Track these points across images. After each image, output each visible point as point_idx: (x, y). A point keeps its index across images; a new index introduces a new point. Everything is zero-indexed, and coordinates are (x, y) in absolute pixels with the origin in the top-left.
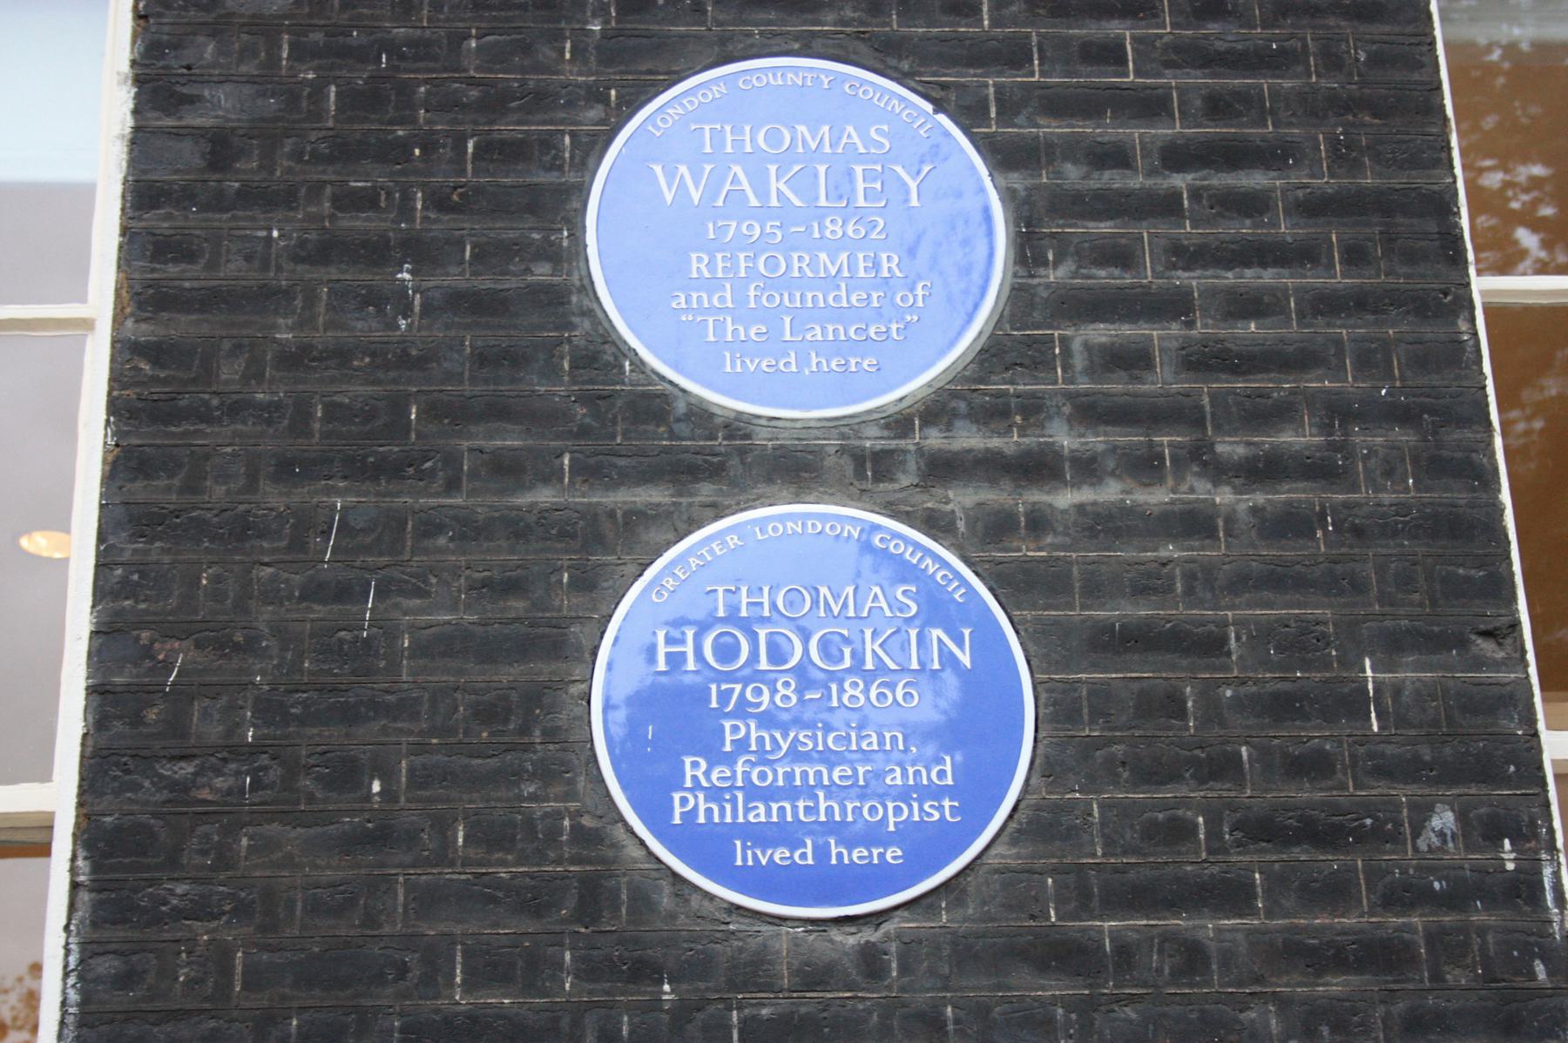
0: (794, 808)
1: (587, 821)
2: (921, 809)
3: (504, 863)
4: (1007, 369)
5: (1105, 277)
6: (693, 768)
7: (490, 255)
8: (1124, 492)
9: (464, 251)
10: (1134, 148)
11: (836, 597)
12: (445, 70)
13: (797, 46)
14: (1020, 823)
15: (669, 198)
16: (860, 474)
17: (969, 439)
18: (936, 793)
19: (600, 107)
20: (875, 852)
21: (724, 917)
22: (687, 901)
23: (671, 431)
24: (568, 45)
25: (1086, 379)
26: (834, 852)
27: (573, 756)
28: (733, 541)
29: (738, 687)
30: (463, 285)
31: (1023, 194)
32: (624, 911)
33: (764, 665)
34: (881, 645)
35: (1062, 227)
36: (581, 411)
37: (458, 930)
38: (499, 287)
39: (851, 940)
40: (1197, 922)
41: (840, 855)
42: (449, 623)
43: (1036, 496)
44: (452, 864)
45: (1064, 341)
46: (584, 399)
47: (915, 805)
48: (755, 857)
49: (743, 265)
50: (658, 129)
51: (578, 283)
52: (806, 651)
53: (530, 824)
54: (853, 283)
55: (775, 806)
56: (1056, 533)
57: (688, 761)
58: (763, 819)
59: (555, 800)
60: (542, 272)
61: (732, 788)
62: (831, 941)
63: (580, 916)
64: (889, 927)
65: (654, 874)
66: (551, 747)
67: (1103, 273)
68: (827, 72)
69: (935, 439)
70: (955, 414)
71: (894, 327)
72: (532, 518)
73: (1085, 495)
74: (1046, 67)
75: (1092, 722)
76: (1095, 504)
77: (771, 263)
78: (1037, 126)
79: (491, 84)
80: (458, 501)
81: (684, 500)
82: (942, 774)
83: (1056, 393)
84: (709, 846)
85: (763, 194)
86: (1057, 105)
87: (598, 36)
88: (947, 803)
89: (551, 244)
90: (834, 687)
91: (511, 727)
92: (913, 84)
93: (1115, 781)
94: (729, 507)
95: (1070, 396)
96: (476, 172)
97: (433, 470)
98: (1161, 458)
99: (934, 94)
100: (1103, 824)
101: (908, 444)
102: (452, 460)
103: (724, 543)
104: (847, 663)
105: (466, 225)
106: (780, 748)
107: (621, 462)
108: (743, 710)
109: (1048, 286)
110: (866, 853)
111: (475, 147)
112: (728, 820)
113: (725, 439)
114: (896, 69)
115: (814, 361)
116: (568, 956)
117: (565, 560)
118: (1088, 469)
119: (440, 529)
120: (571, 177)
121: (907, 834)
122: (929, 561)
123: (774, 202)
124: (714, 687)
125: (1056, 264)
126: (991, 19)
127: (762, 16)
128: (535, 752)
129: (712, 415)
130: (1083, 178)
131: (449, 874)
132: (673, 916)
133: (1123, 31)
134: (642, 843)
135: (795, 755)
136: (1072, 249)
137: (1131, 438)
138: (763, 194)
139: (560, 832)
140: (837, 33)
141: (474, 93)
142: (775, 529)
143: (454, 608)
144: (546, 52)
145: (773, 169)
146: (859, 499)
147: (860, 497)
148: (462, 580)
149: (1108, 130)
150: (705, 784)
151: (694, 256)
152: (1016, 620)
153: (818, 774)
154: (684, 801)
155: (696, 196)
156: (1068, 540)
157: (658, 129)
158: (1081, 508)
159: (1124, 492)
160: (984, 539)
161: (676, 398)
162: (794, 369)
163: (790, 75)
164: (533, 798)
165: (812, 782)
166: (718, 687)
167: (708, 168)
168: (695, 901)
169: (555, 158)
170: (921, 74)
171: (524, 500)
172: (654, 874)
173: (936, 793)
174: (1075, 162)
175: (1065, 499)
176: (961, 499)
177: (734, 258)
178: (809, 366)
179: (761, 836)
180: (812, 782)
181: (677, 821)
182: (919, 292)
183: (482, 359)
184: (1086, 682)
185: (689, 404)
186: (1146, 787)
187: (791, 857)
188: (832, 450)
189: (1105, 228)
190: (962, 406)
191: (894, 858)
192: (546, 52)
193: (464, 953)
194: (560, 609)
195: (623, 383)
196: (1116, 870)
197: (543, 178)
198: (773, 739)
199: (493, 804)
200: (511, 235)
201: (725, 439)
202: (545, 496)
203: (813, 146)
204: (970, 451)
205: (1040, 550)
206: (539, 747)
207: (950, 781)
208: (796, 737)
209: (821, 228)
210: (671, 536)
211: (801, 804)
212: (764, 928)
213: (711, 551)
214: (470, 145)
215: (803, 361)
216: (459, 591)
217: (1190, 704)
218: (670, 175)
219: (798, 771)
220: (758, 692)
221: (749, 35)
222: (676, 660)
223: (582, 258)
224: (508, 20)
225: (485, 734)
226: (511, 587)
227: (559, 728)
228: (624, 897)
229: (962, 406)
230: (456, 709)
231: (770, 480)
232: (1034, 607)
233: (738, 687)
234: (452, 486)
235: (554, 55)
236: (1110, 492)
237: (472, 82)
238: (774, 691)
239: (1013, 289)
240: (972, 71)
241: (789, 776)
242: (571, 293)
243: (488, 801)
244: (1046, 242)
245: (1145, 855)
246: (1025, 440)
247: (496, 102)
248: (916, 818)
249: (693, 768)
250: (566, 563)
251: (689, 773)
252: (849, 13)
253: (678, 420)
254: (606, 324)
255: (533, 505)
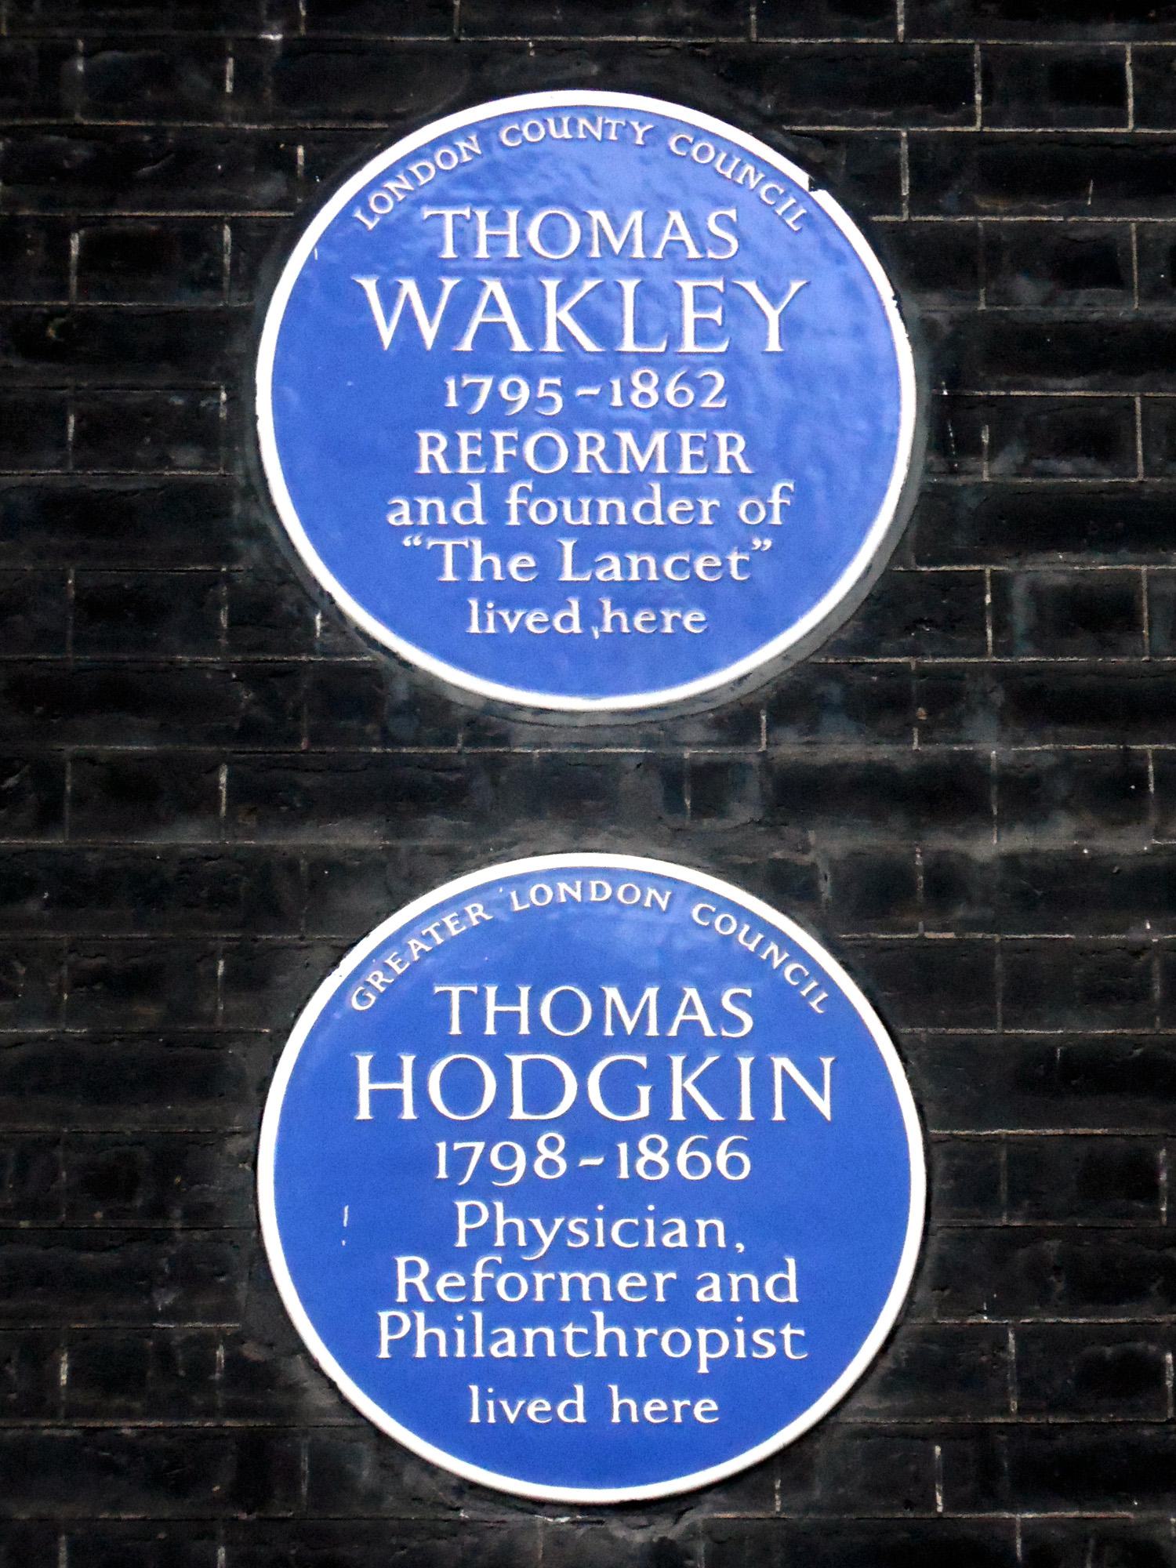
0: (560, 1338)
1: (252, 1352)
2: (749, 1340)
3: (128, 1413)
4: (908, 630)
5: (1070, 473)
6: (410, 1272)
7: (106, 433)
8: (1078, 835)
9: (65, 422)
10: (1129, 249)
11: (631, 1008)
12: (36, 112)
13: (595, 70)
14: (896, 1360)
15: (387, 334)
16: (673, 803)
17: (844, 747)
18: (770, 1314)
19: (279, 176)
20: (678, 1405)
21: (451, 1499)
22: (398, 1475)
23: (385, 731)
24: (230, 67)
25: (1029, 648)
26: (617, 1403)
27: (230, 1250)
28: (476, 913)
29: (479, 1147)
30: (64, 484)
31: (947, 330)
32: (304, 1489)
33: (518, 1113)
34: (696, 1083)
35: (1008, 386)
36: (247, 696)
37: (62, 1512)
38: (121, 487)
39: (639, 1537)
40: (1154, 1514)
41: (625, 1410)
42: (43, 1038)
43: (943, 841)
44: (52, 1414)
45: (1001, 584)
46: (255, 676)
47: (740, 1333)
48: (499, 1409)
49: (500, 452)
50: (371, 215)
51: (242, 482)
52: (583, 1091)
53: (165, 1354)
54: (673, 487)
55: (530, 1333)
56: (970, 900)
57: (402, 1261)
58: (511, 1352)
59: (205, 1319)
60: (186, 464)
61: (469, 1305)
62: (612, 1539)
63: (239, 1495)
64: (695, 1517)
65: (349, 1433)
66: (198, 1235)
67: (1066, 466)
68: (644, 116)
69: (790, 747)
70: (823, 704)
71: (734, 558)
72: (171, 871)
73: (1019, 840)
74: (995, 105)
75: (1014, 1203)
76: (1034, 853)
77: (545, 452)
78: (974, 211)
79: (111, 134)
80: (56, 841)
81: (403, 844)
82: (781, 1286)
83: (978, 670)
84: (426, 1390)
85: (533, 330)
86: (1012, 173)
87: (278, 52)
88: (787, 1331)
89: (199, 413)
90: (623, 1147)
91: (139, 1203)
92: (779, 138)
93: (1043, 1297)
94: (472, 855)
95: (1004, 675)
96: (84, 289)
97: (18, 789)
98: (1141, 779)
99: (811, 155)
100: (1020, 1363)
101: (748, 755)
102: (47, 775)
103: (463, 914)
104: (644, 1111)
105: (68, 381)
106: (540, 1243)
107: (308, 781)
108: (486, 1184)
109: (980, 487)
110: (663, 1407)
111: (84, 246)
112: (461, 1353)
113: (466, 744)
114: (753, 110)
115: (608, 616)
116: (222, 1553)
117: (223, 938)
118: (1026, 796)
119: (30, 887)
120: (234, 300)
121: (729, 1378)
122: (773, 947)
123: (552, 345)
124: (442, 1146)
125: (996, 447)
126: (907, 23)
127: (540, 17)
128: (172, 1243)
129: (448, 704)
130: (1044, 304)
131: (47, 1429)
132: (375, 1497)
133: (1122, 44)
134: (332, 1385)
135: (562, 1256)
136: (1020, 425)
137: (1092, 746)
138: (533, 330)
139: (212, 1363)
140: (657, 46)
141: (81, 152)
142: (541, 893)
143: (51, 1014)
144: (195, 80)
145: (551, 285)
146: (670, 845)
147: (673, 845)
148: (65, 971)
149: (1091, 219)
150: (426, 1297)
151: (424, 436)
152: (903, 1041)
153: (596, 1284)
154: (395, 1324)
155: (429, 333)
156: (990, 913)
157: (371, 215)
158: (1011, 861)
159: (1078, 835)
160: (856, 909)
161: (394, 675)
162: (576, 628)
163: (583, 122)
164: (170, 1314)
165: (586, 1297)
166: (450, 1146)
167: (449, 284)
168: (409, 1476)
169: (207, 266)
170: (790, 119)
171: (156, 841)
172: (349, 1433)
173: (770, 1314)
174: (1031, 272)
175: (989, 846)
176: (828, 845)
177: (489, 445)
178: (600, 623)
179: (515, 1377)
180: (586, 1297)
181: (384, 1353)
182: (776, 500)
183: (95, 607)
184: (1007, 1140)
185: (412, 685)
186: (1089, 1307)
187: (553, 1412)
188: (632, 763)
189: (1074, 389)
190: (834, 691)
191: (705, 1414)
192: (195, 80)
193: (73, 1548)
194: (211, 1019)
195: (311, 651)
196: (1037, 1432)
197: (188, 301)
198: (530, 1230)
199: (111, 1322)
200: (137, 397)
201: (466, 744)
202: (190, 836)
203: (617, 246)
204: (843, 766)
205: (945, 928)
206: (178, 1235)
207: (793, 1298)
208: (564, 1227)
209: (627, 389)
210: (380, 903)
211: (569, 1330)
212: (512, 1517)
213: (442, 929)
214: (75, 242)
215: (591, 617)
216: (60, 989)
217: (1163, 1177)
218: (388, 295)
219: (566, 1278)
220: (508, 1155)
221: (521, 49)
222: (386, 1102)
223: (248, 438)
224: (136, 24)
225: (99, 1215)
226: (132, 982)
227: (210, 1207)
228: (305, 1467)
229: (834, 691)
230: (55, 1176)
231: (534, 811)
232: (933, 1022)
233: (479, 1147)
234: (48, 817)
235: (206, 85)
236: (1058, 836)
237: (78, 133)
238: (532, 1153)
239: (923, 494)
240: (875, 114)
241: (552, 1287)
242: (231, 498)
243: (105, 1318)
244: (979, 413)
245: (1082, 1412)
246: (929, 748)
247: (114, 169)
248: (741, 1353)
249: (410, 1272)
250: (223, 945)
251: (403, 1280)
252: (683, 13)
253: (397, 712)
254: (285, 553)
255: (170, 852)
